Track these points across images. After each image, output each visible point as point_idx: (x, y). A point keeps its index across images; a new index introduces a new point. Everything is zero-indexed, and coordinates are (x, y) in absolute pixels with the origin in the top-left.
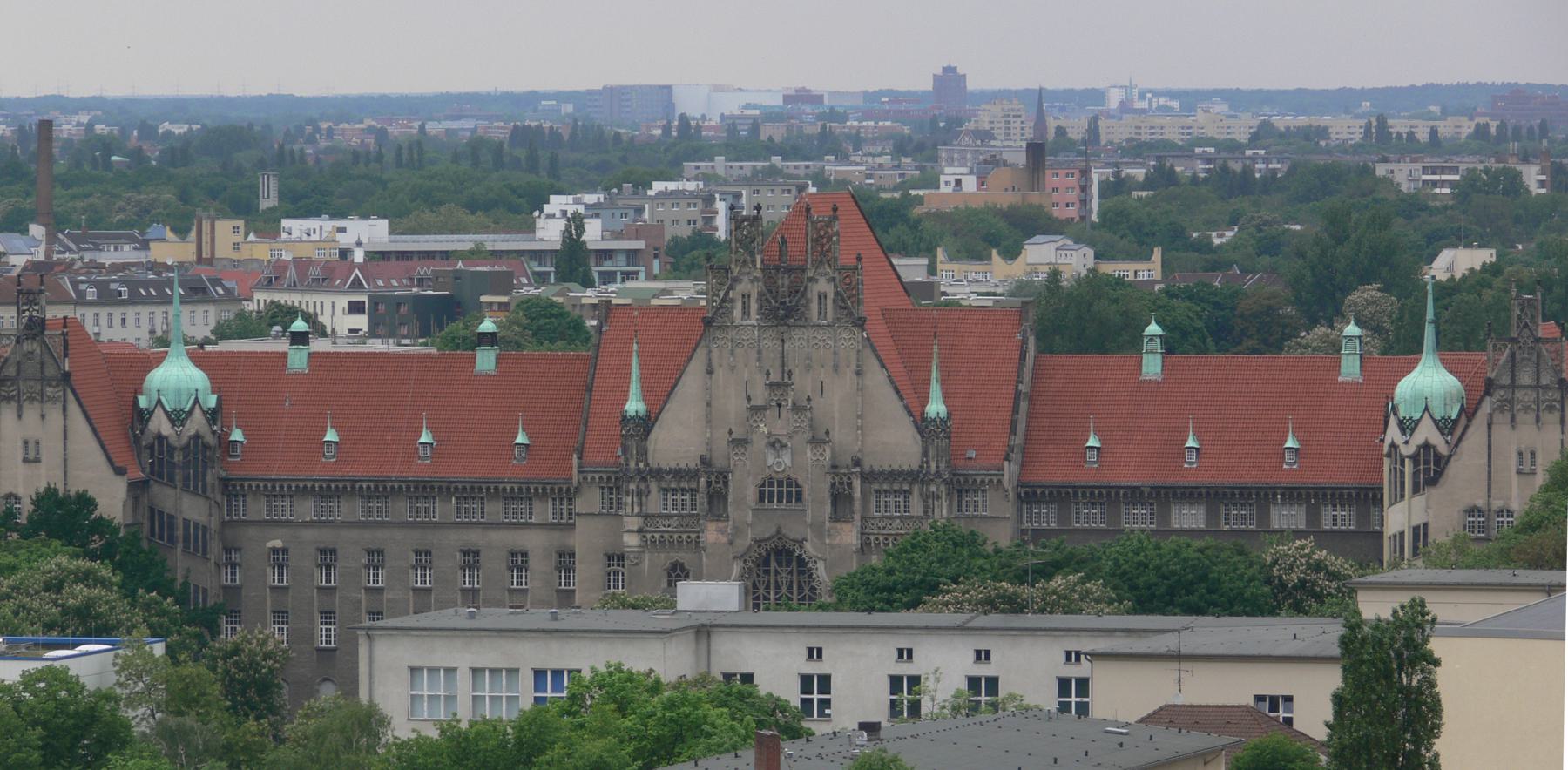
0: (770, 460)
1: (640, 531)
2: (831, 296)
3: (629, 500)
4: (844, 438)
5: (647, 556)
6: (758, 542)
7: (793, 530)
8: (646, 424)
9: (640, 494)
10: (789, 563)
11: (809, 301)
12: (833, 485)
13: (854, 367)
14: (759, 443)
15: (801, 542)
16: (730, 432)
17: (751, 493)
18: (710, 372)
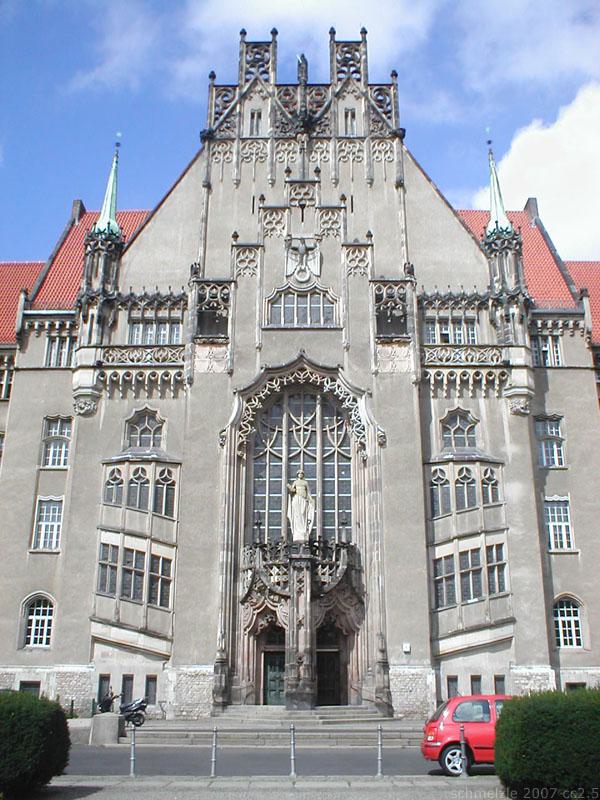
0: (292, 266)
1: (99, 365)
2: (361, 107)
3: (87, 327)
4: (387, 260)
5: (104, 403)
6: (270, 372)
7: (322, 352)
8: (116, 247)
9: (102, 321)
10: (311, 410)
11: (335, 114)
12: (379, 298)
13: (393, 180)
14: (275, 247)
15: (332, 372)
16: (236, 236)
17: (259, 309)
18: (208, 186)
